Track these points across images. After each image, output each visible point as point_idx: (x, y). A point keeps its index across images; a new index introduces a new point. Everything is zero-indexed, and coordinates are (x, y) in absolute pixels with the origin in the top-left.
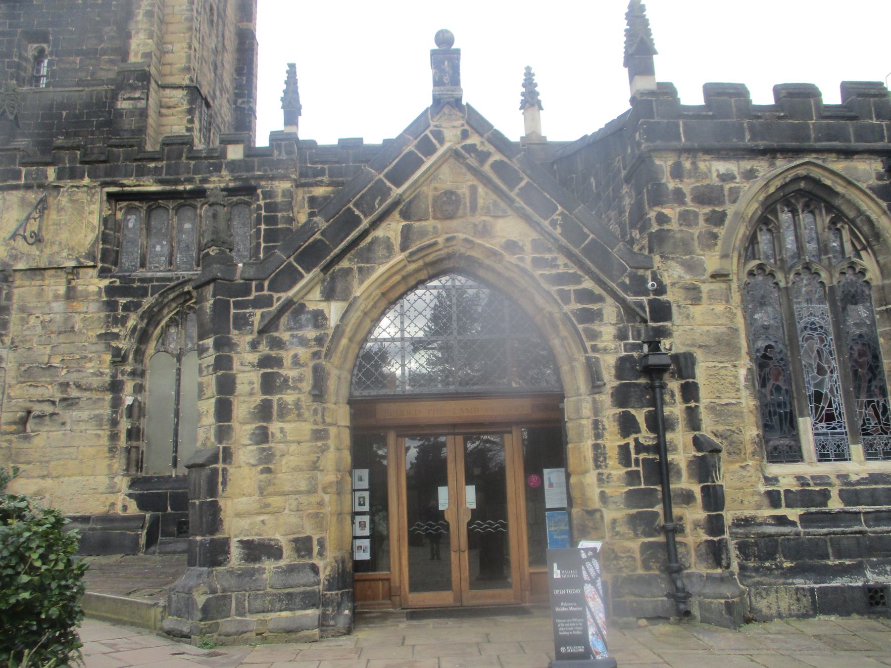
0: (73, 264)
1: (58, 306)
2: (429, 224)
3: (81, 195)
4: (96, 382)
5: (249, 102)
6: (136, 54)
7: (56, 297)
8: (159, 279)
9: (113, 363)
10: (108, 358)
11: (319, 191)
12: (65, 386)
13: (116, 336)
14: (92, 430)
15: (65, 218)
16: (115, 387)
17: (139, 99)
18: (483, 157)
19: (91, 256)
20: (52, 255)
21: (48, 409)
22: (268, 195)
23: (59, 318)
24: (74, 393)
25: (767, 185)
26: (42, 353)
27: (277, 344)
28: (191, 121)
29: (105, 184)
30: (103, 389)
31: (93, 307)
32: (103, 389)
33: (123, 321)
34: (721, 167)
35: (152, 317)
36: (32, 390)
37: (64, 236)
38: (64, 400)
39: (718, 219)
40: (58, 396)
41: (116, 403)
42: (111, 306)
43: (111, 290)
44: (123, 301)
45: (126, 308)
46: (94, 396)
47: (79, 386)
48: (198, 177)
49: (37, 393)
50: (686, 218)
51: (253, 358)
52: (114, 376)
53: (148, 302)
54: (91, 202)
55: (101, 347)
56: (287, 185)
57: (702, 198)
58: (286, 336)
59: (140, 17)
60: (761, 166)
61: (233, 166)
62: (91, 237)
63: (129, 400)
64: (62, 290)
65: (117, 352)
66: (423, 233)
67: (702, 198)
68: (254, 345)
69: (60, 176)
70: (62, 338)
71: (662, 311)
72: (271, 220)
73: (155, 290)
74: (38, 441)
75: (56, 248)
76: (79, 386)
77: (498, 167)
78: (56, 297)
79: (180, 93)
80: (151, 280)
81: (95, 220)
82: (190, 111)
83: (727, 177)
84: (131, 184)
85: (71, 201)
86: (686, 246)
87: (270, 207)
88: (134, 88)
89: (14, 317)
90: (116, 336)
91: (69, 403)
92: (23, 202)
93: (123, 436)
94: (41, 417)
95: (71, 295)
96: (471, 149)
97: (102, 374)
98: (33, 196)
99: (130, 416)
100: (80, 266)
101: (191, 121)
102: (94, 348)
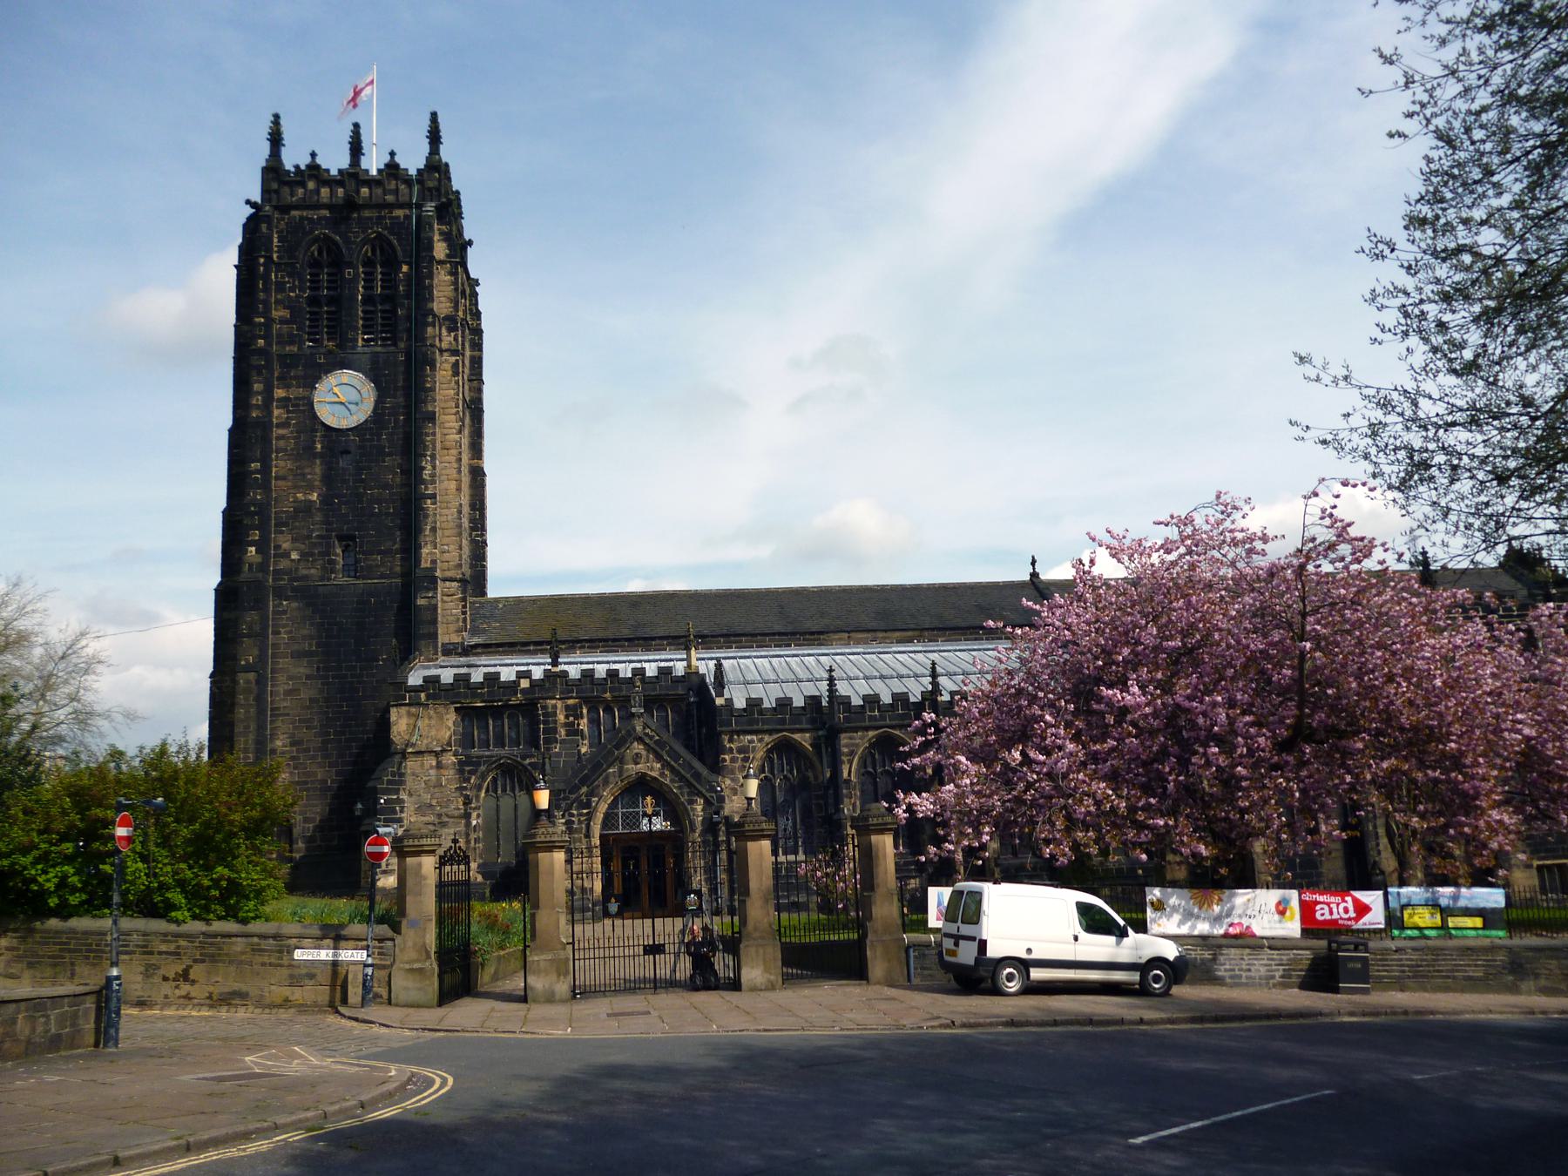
0: (439, 749)
1: (433, 772)
2: (630, 766)
3: (441, 709)
4: (456, 813)
5: (483, 535)
6: (426, 562)
7: (431, 767)
8: (487, 757)
9: (464, 804)
10: (461, 800)
11: (571, 702)
12: (440, 816)
13: (465, 788)
15: (433, 722)
16: (467, 816)
17: (432, 597)
18: (651, 738)
19: (449, 744)
20: (427, 744)
22: (545, 707)
23: (433, 778)
24: (446, 819)
25: (767, 744)
26: (427, 797)
27: (573, 815)
28: (465, 607)
29: (453, 703)
30: (460, 817)
31: (452, 772)
32: (460, 817)
33: (468, 780)
34: (749, 737)
35: (483, 777)
36: (423, 818)
37: (433, 733)
38: (439, 823)
39: (746, 759)
40: (437, 821)
41: (468, 824)
42: (461, 772)
43: (460, 763)
44: (467, 768)
45: (470, 772)
46: (456, 820)
47: (447, 816)
48: (505, 698)
49: (426, 819)
50: (733, 760)
51: (563, 821)
52: (465, 810)
53: (483, 768)
54: (447, 713)
55: (458, 794)
56: (554, 702)
57: (740, 751)
58: (575, 812)
59: (427, 533)
60: (767, 738)
61: (524, 691)
62: (448, 734)
63: (474, 823)
64: (434, 763)
65: (467, 797)
66: (628, 770)
67: (740, 751)
68: (563, 816)
69: (428, 697)
70: (436, 790)
71: (721, 799)
72: (545, 723)
73: (485, 762)
75: (430, 740)
76: (447, 816)
77: (656, 742)
78: (431, 767)
79: (455, 584)
80: (482, 757)
81: (450, 724)
82: (464, 599)
83: (750, 742)
84: (467, 702)
85: (436, 713)
86: (733, 772)
87: (545, 715)
88: (428, 589)
89: (409, 779)
90: (465, 788)
91: (443, 825)
92: (409, 714)
93: (473, 842)
95: (439, 766)
96: (647, 734)
97: (459, 809)
98: (413, 710)
99: (475, 831)
100: (444, 751)
101: (465, 607)
102: (454, 795)
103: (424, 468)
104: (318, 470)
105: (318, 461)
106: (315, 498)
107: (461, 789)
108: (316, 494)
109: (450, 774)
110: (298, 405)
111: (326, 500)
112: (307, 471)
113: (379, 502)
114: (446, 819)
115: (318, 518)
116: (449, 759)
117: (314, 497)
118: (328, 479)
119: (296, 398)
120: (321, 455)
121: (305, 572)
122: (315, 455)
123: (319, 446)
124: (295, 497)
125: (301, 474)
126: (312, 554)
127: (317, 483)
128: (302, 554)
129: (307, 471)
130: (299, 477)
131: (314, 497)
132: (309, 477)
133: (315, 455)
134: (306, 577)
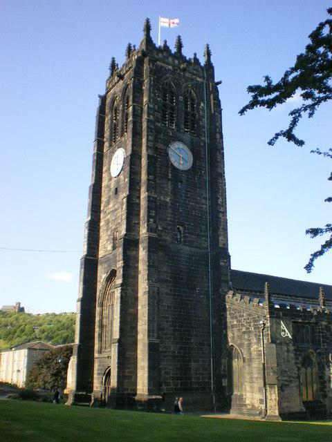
10: (296, 369)
14: (295, 388)
21: (287, 383)
24: (292, 379)
33: (298, 359)
42: (296, 354)
45: (299, 355)
49: (284, 379)
74: (286, 392)
91: (291, 381)
94: (286, 385)
103: (219, 198)
104: (169, 187)
105: (170, 182)
107: (296, 363)
109: (292, 355)
111: (173, 202)
112: (166, 186)
113: (195, 210)
114: (292, 379)
116: (292, 348)
117: (168, 200)
121: (164, 237)
122: (169, 180)
127: (170, 193)
128: (163, 228)
129: (166, 186)
131: (168, 200)
133: (169, 180)
134: (165, 240)
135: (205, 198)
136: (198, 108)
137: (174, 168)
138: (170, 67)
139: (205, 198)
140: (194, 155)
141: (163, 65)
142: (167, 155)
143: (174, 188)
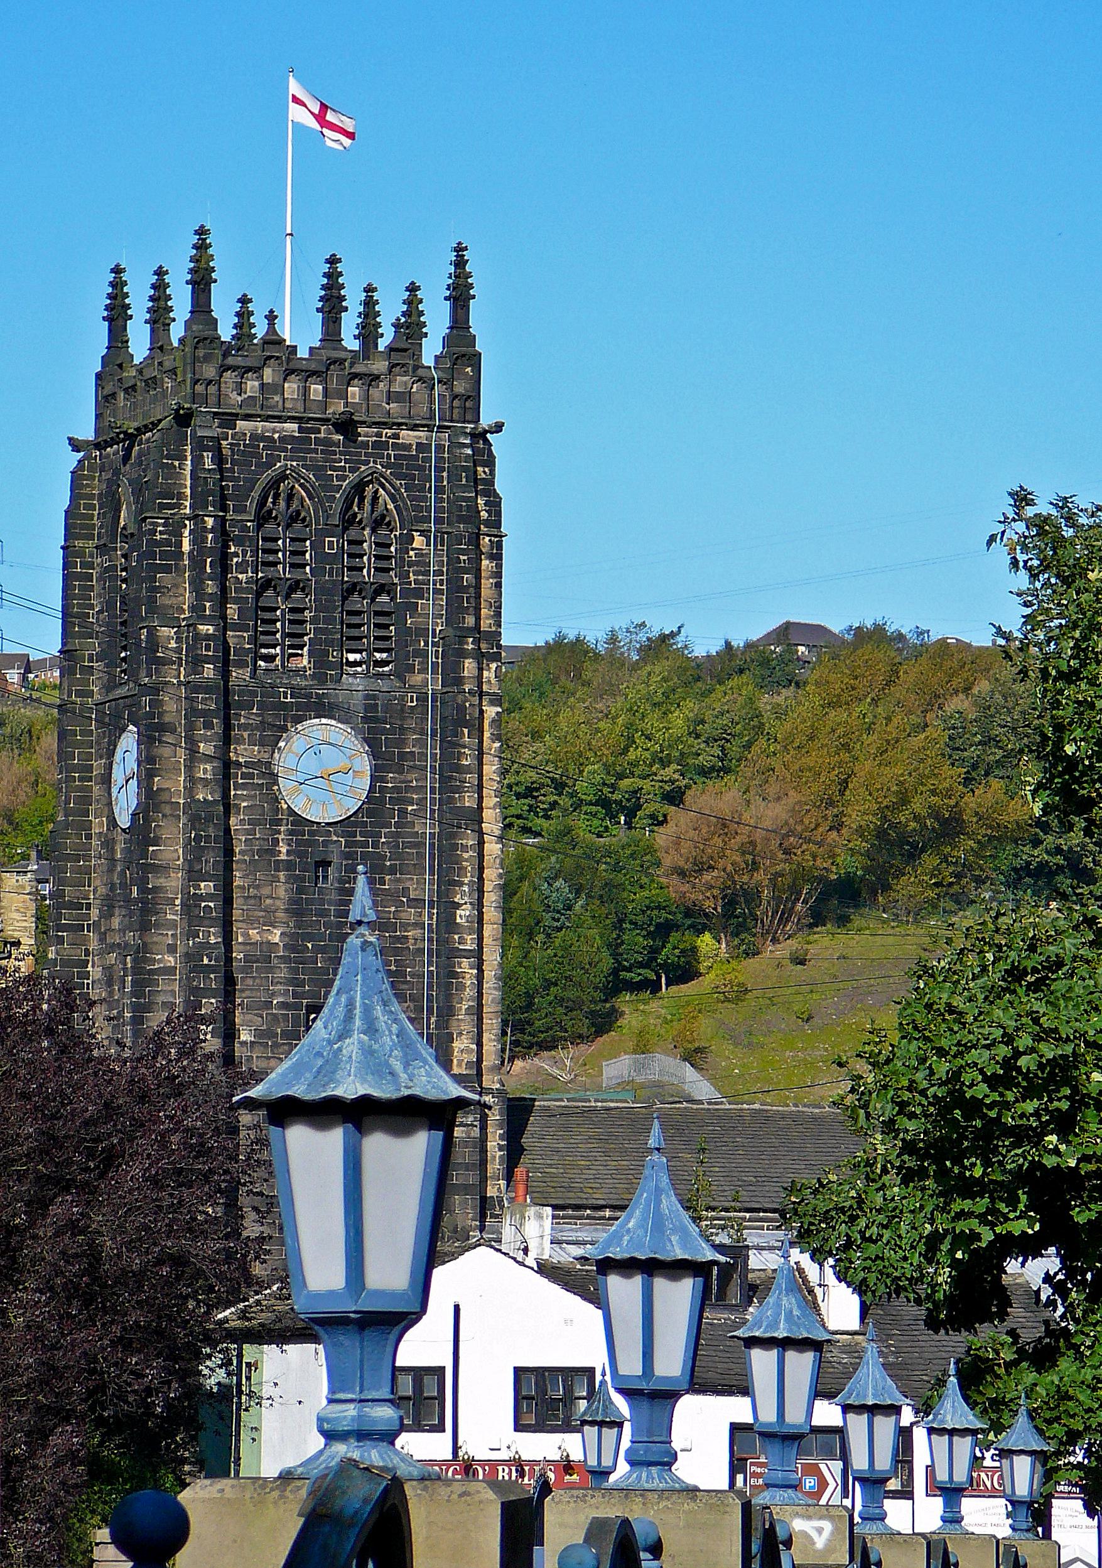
103: (458, 906)
104: (282, 891)
105: (282, 875)
106: (276, 940)
108: (278, 933)
110: (251, 776)
111: (294, 944)
115: (283, 973)
117: (276, 936)
118: (297, 909)
119: (248, 765)
120: (289, 866)
123: (284, 850)
124: (246, 935)
125: (255, 897)
126: (273, 1035)
127: (280, 915)
128: (259, 1033)
129: (266, 891)
130: (252, 901)
131: (276, 936)
132: (268, 901)
135: (417, 902)
136: (401, 562)
137: (299, 821)
138: (292, 427)
139: (417, 902)
140: (375, 754)
141: (260, 426)
142: (273, 778)
143: (301, 890)
